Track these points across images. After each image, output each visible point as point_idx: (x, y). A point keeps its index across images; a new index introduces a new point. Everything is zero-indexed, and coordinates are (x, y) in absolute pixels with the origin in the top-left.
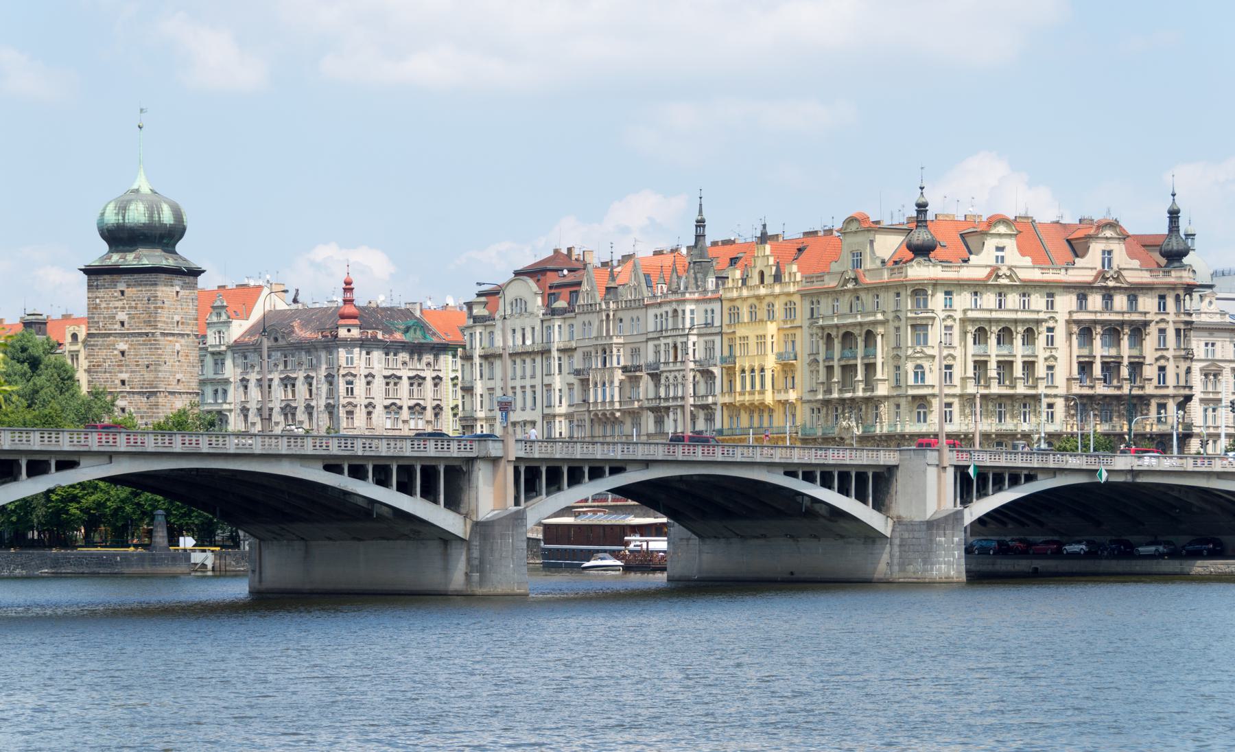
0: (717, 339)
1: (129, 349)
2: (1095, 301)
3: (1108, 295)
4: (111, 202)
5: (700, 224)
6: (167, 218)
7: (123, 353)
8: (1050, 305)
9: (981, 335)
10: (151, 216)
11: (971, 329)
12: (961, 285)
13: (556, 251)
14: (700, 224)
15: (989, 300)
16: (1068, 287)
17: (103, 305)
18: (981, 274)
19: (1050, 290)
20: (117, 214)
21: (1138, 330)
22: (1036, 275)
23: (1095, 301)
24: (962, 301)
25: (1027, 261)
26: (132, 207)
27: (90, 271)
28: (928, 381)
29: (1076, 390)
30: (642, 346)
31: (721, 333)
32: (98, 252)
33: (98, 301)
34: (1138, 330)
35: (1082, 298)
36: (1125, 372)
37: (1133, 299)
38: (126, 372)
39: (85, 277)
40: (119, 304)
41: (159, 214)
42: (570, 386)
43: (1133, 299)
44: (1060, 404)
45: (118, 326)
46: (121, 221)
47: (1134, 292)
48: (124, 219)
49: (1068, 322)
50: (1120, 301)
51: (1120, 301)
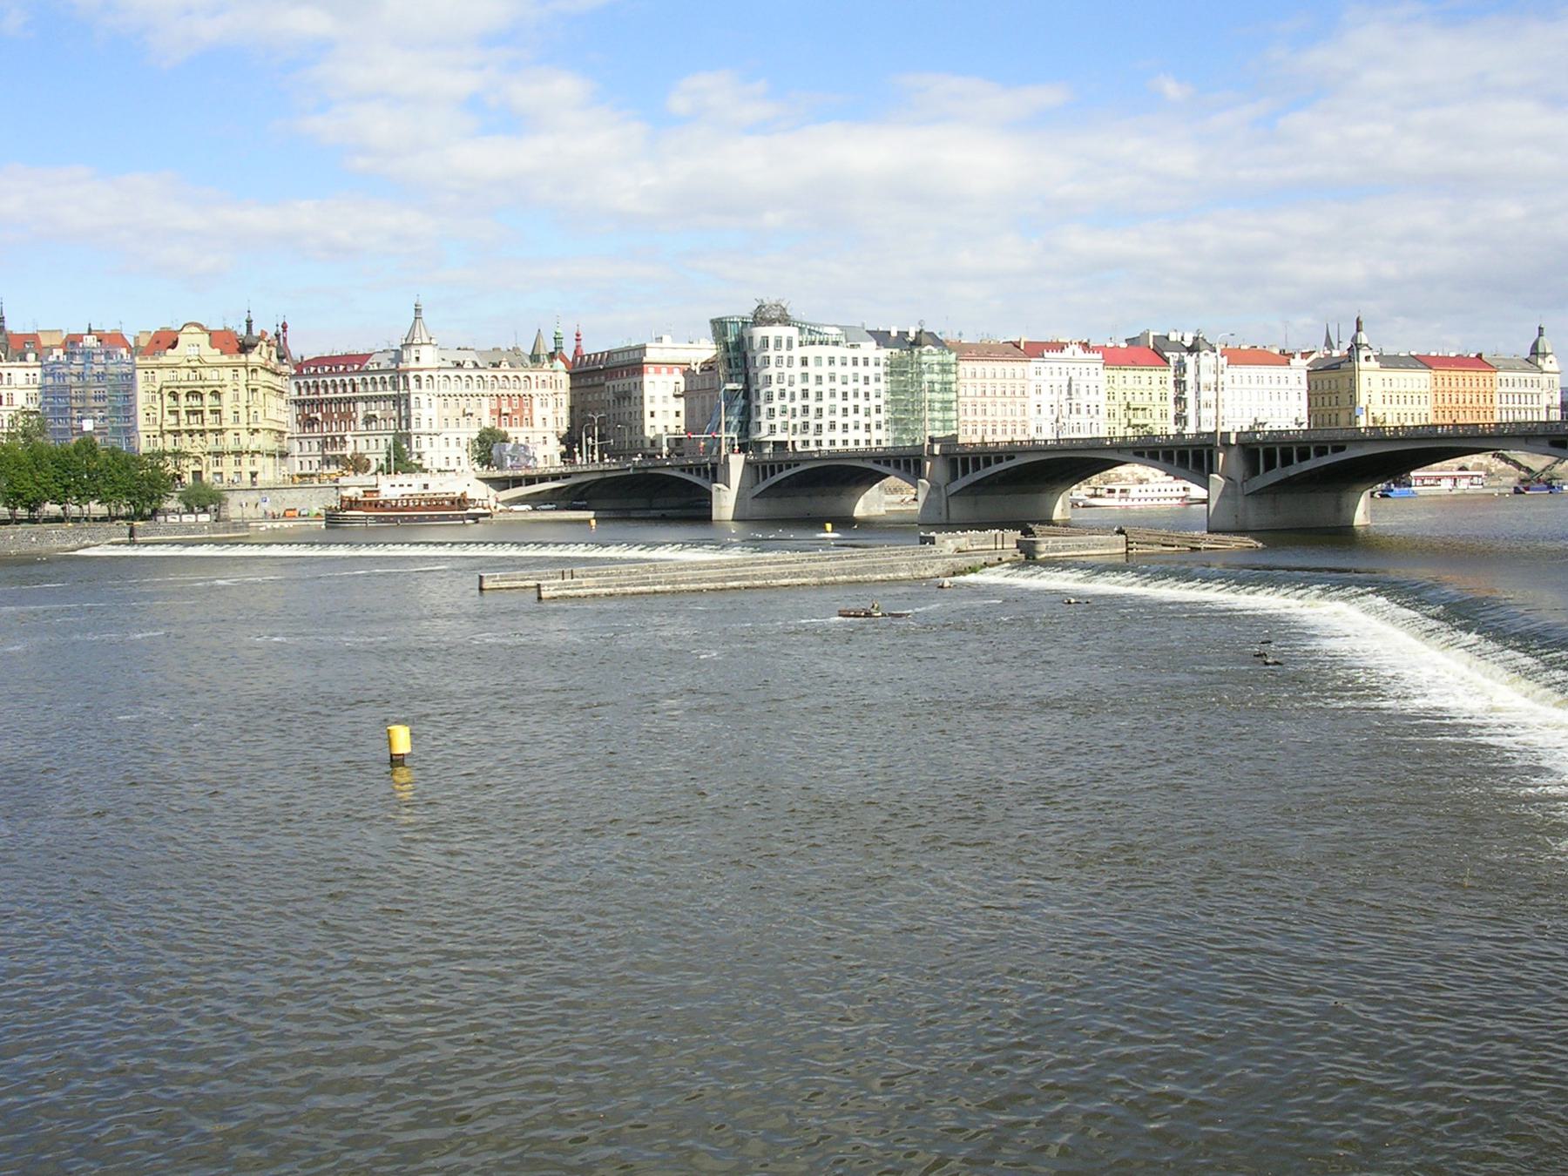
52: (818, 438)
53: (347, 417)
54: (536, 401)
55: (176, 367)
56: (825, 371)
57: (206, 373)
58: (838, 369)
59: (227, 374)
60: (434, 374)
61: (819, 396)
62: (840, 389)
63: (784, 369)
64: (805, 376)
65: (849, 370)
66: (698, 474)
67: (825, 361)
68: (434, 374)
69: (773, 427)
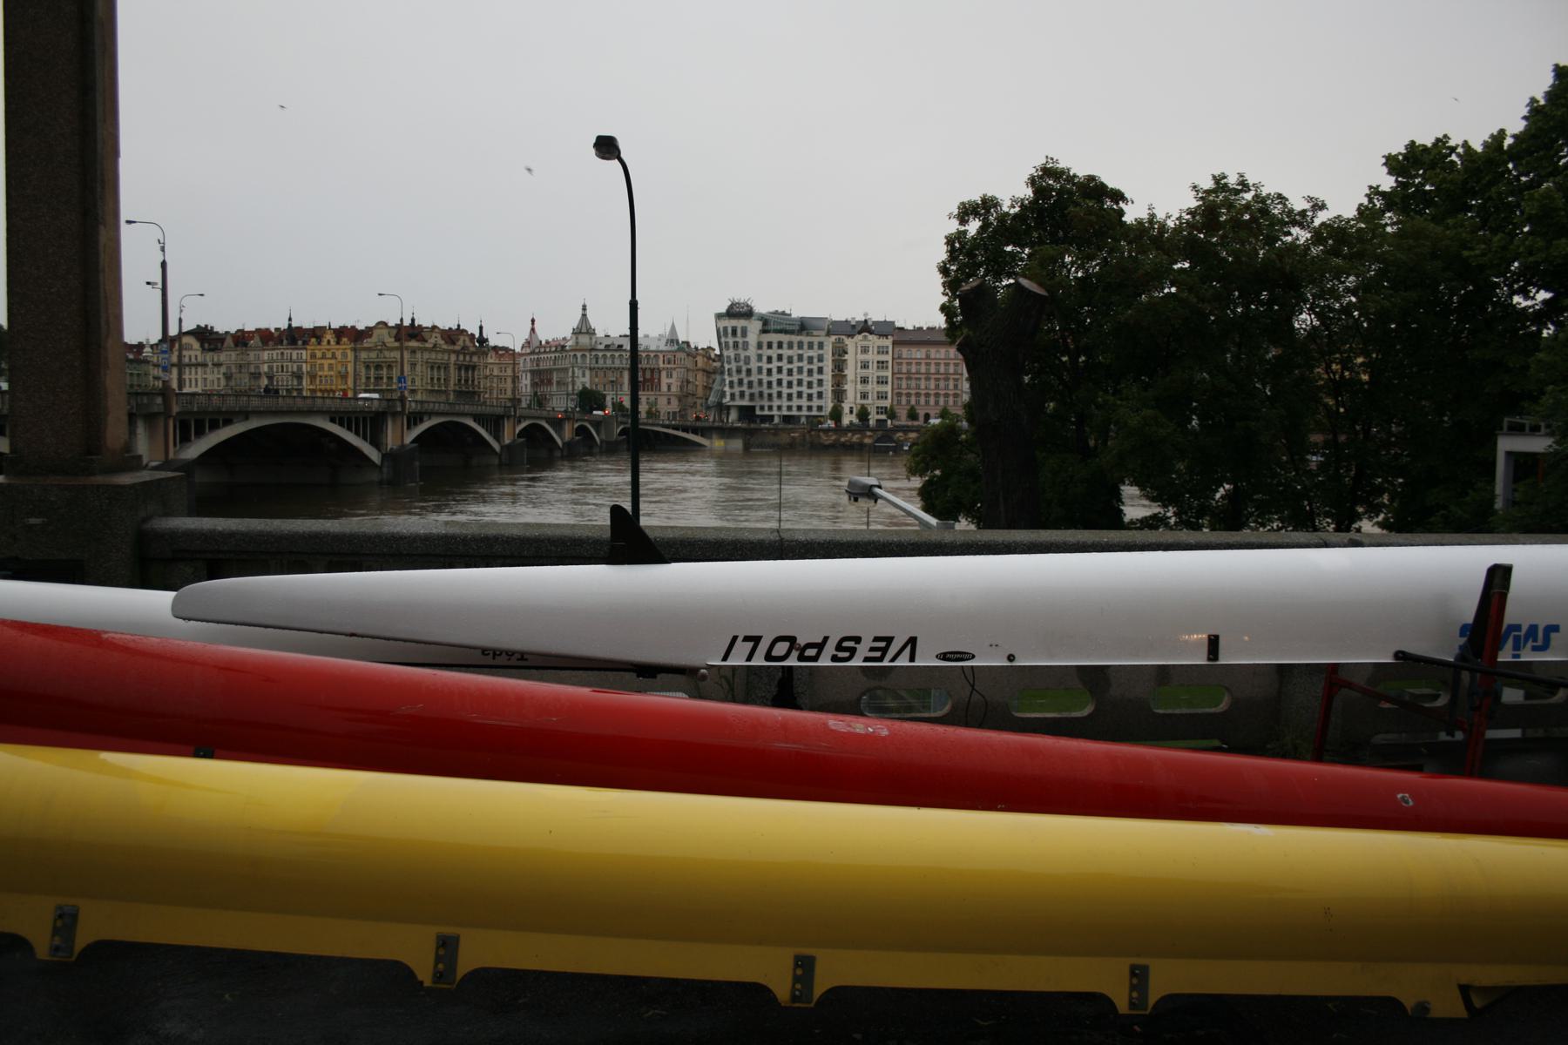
0: (304, 365)
2: (461, 358)
3: (465, 354)
5: (290, 319)
8: (449, 358)
9: (432, 368)
11: (430, 365)
12: (426, 349)
13: (198, 326)
14: (290, 319)
15: (433, 356)
16: (454, 352)
18: (431, 346)
19: (450, 352)
21: (474, 368)
22: (445, 347)
23: (461, 358)
24: (426, 355)
25: (443, 342)
28: (416, 384)
29: (457, 388)
30: (261, 366)
31: (306, 362)
34: (474, 368)
35: (458, 356)
36: (470, 382)
37: (471, 357)
42: (219, 379)
43: (471, 357)
44: (452, 393)
47: (472, 354)
49: (455, 364)
50: (468, 358)
51: (468, 358)
52: (770, 404)
53: (550, 382)
54: (664, 374)
55: (369, 349)
56: (774, 353)
57: (387, 354)
58: (786, 352)
59: (397, 354)
60: (587, 354)
61: (769, 371)
62: (786, 366)
63: (740, 351)
64: (760, 357)
65: (794, 352)
66: (341, 424)
67: (775, 345)
68: (587, 354)
69: (733, 396)
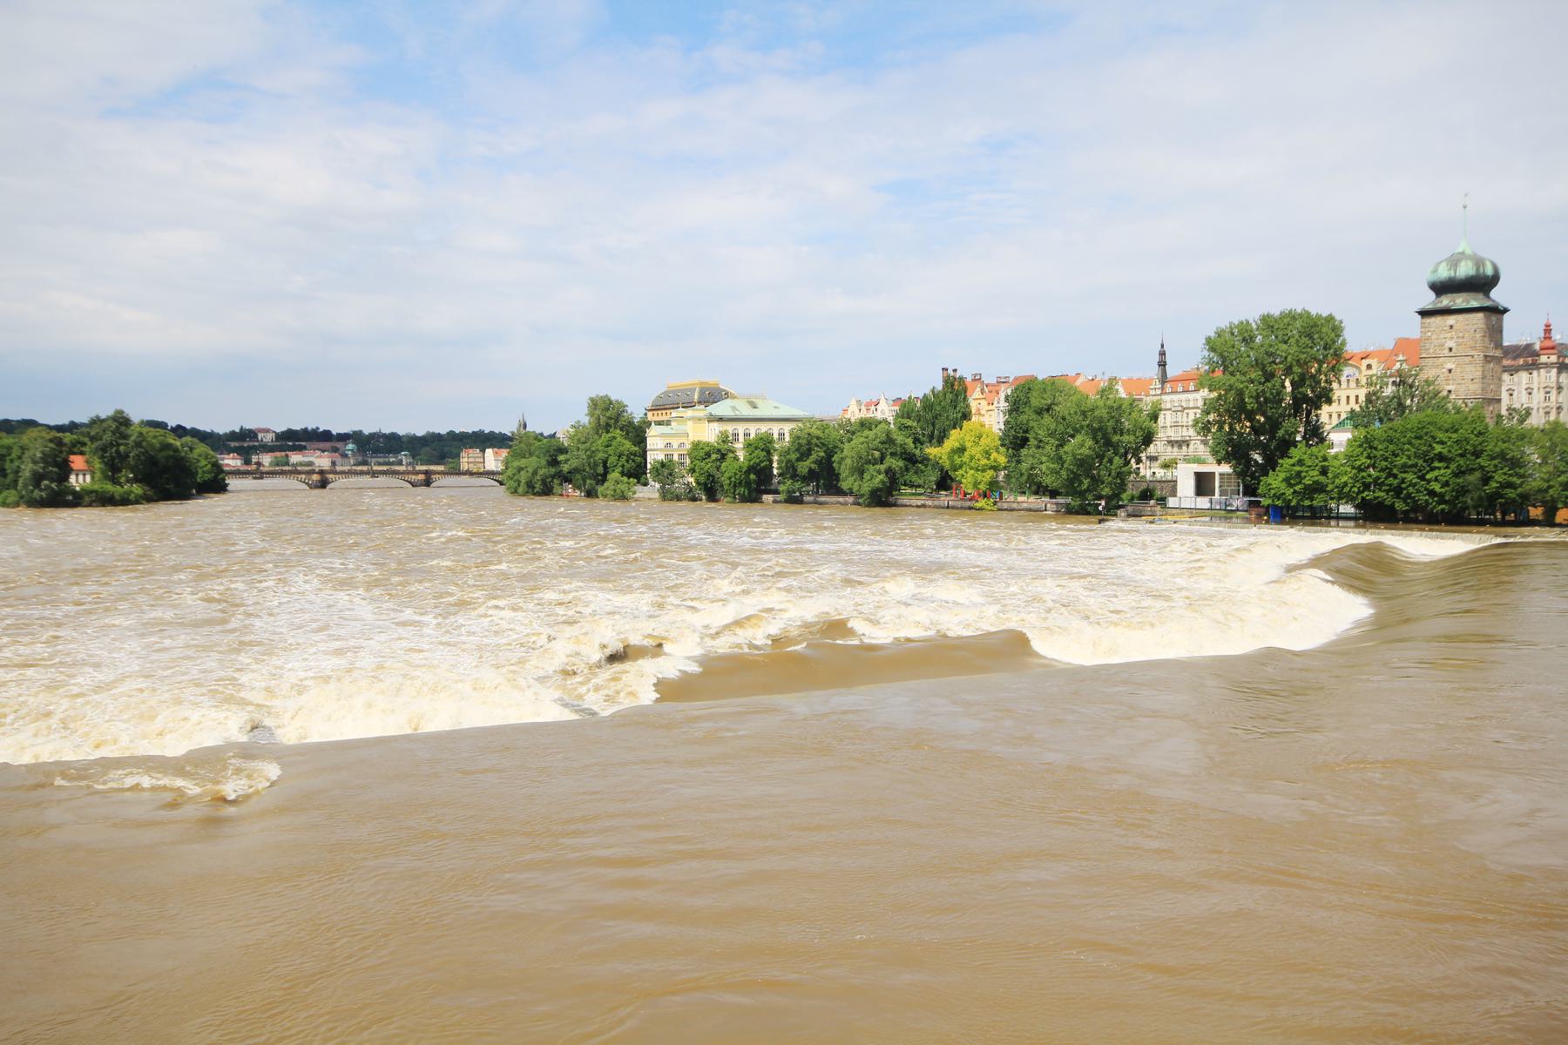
1: (1456, 367)
4: (1441, 262)
6: (1489, 271)
7: (1450, 371)
10: (1478, 269)
17: (1434, 337)
20: (1450, 269)
26: (1463, 264)
27: (1424, 314)
32: (1428, 299)
33: (1429, 334)
38: (1453, 384)
39: (1420, 317)
40: (1449, 335)
41: (1484, 268)
45: (1446, 351)
46: (1453, 275)
48: (1455, 273)
